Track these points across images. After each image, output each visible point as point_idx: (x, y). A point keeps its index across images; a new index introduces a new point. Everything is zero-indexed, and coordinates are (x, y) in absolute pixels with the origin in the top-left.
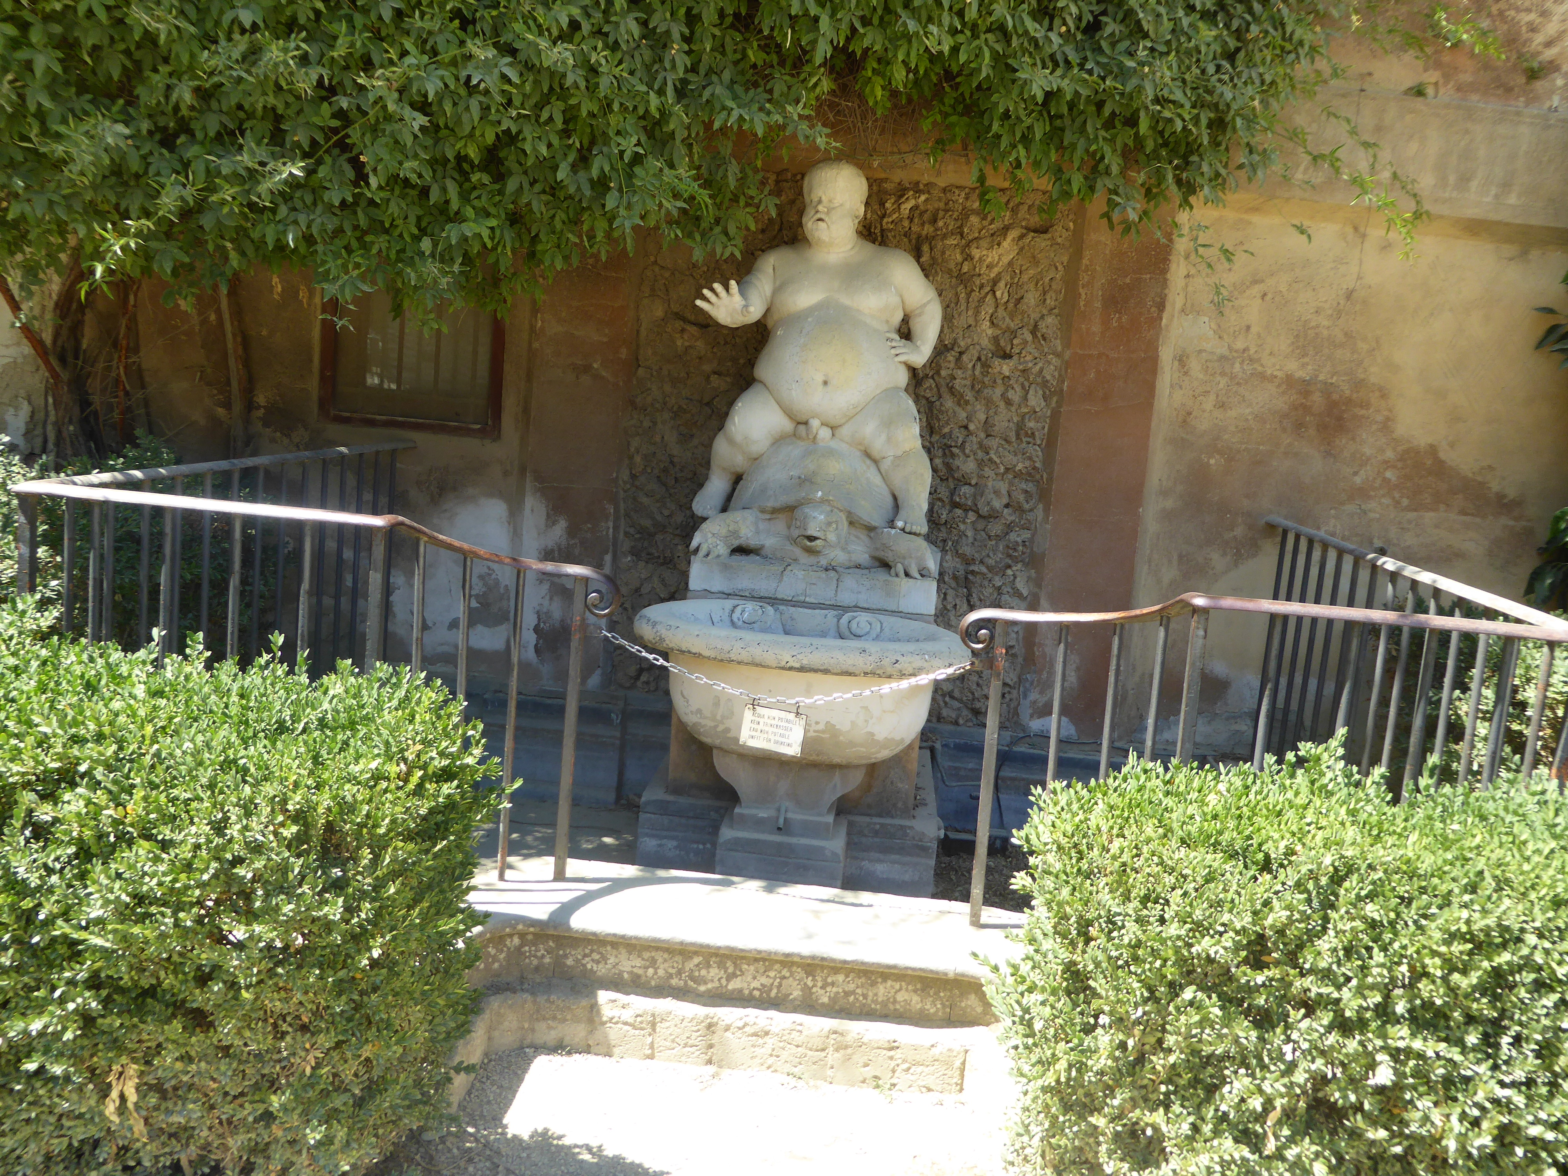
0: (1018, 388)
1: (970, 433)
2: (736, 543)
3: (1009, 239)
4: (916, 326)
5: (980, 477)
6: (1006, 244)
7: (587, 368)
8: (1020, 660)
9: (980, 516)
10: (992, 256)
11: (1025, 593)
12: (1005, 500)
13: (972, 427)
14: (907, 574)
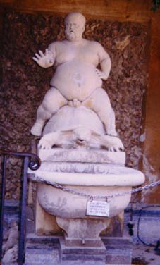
1: (117, 102)
4: (103, 65)
12: (130, 125)
13: (118, 100)
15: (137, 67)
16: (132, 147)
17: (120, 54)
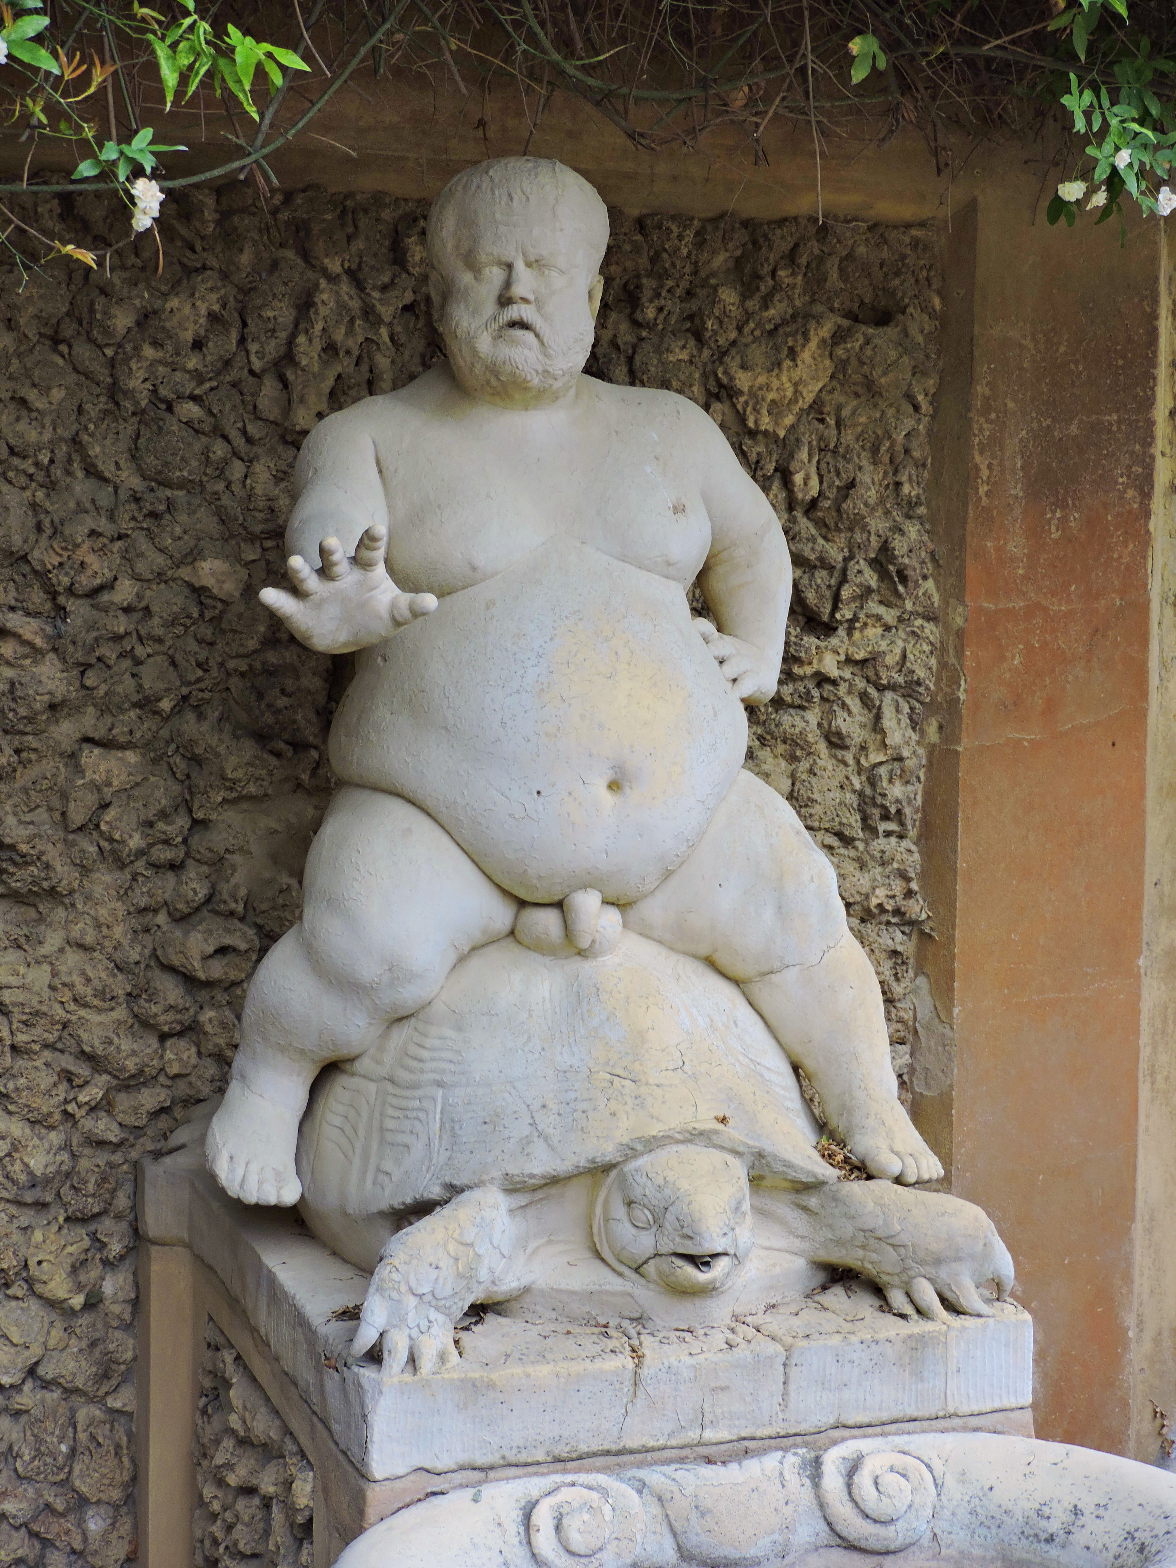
0: (854, 703)
6: (806, 356)
10: (782, 384)
14: (951, 1307)
15: (883, 560)
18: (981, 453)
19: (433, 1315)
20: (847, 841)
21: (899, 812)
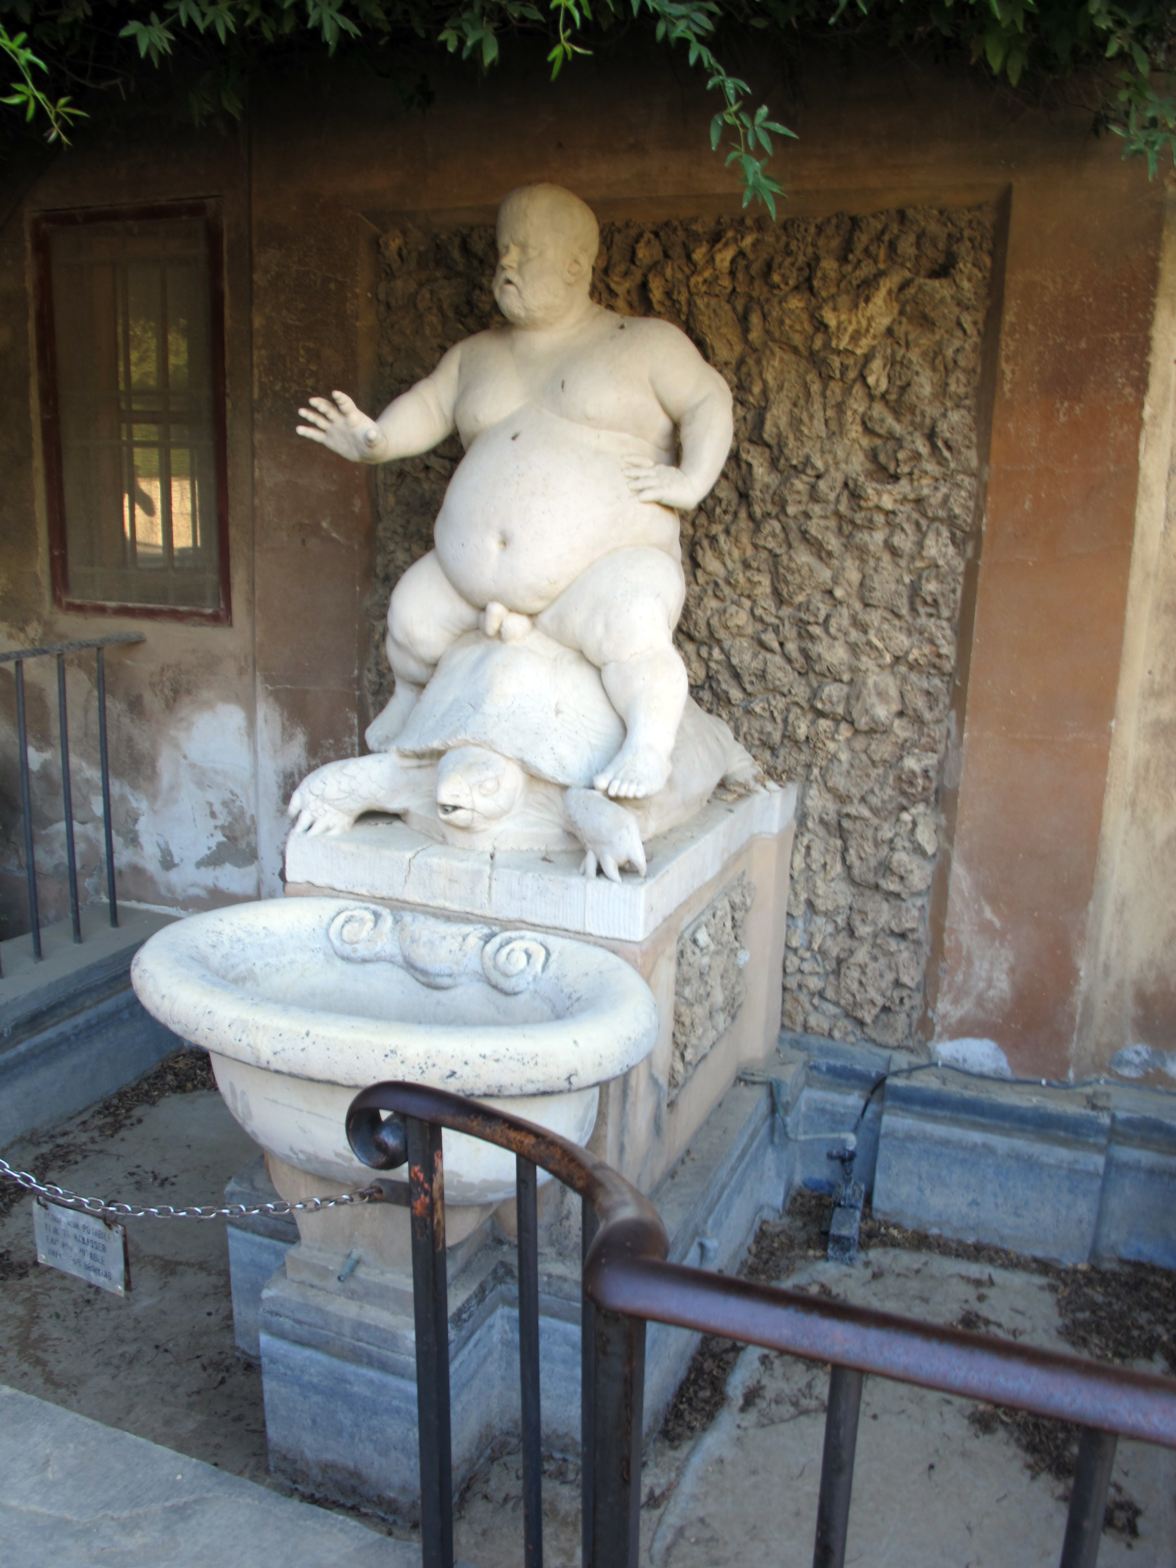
2: (359, 807)
3: (883, 292)
5: (854, 670)
7: (316, 530)
8: (926, 949)
9: (856, 732)
11: (930, 850)
12: (895, 707)
13: (839, 593)
15: (931, 436)
16: (904, 809)
17: (852, 374)
18: (1007, 362)
19: (327, 807)
20: (898, 616)
21: (935, 601)
